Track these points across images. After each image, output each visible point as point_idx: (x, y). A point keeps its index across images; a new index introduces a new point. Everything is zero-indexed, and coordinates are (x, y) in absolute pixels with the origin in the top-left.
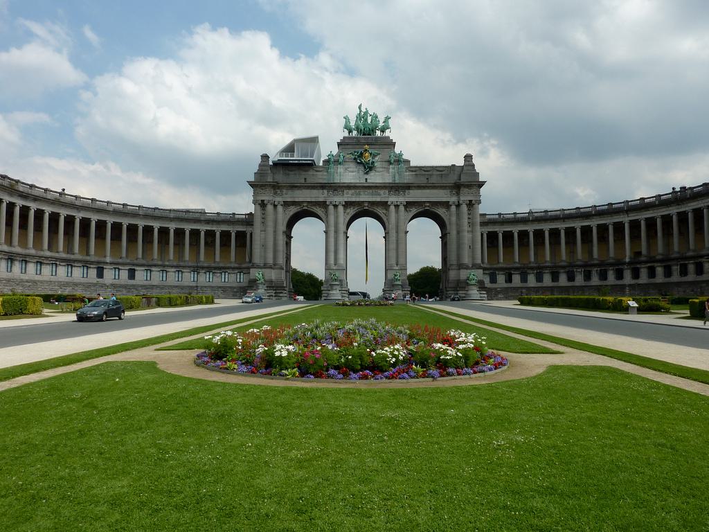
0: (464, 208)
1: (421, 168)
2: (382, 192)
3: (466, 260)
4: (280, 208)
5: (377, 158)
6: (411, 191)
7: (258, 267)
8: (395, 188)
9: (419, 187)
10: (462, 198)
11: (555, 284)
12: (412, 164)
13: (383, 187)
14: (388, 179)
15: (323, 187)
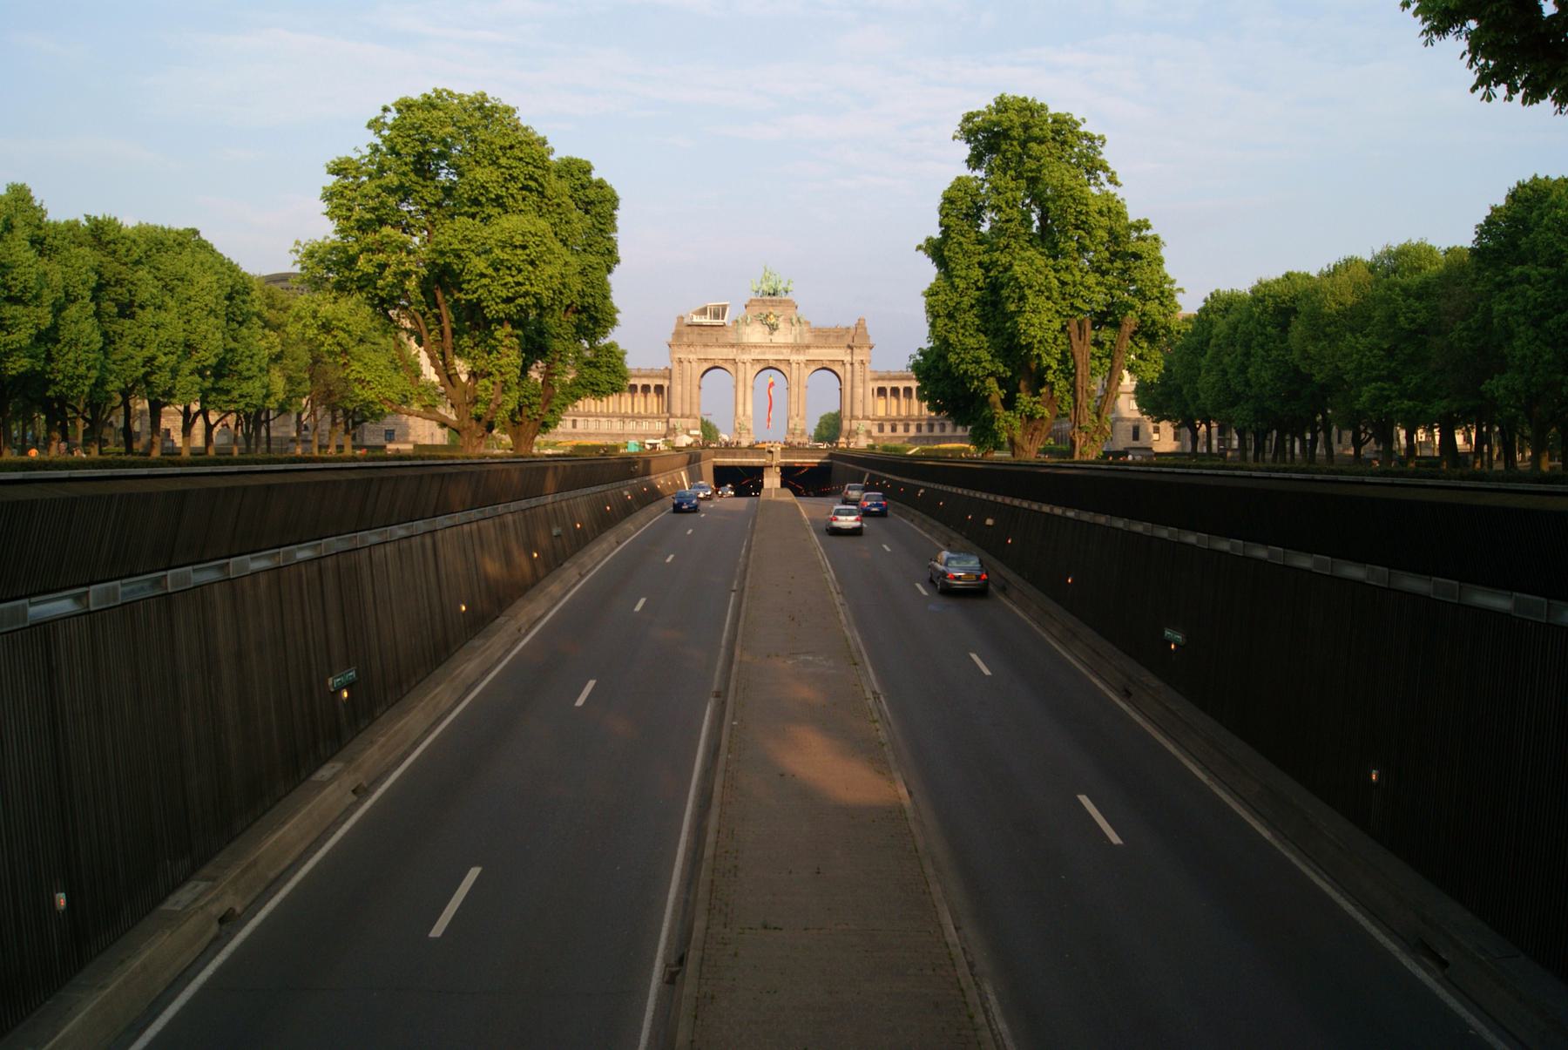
0: (857, 366)
1: (819, 330)
2: (785, 351)
3: (859, 412)
4: (694, 364)
5: (781, 319)
6: (811, 351)
7: (676, 417)
8: (797, 347)
9: (817, 347)
10: (855, 358)
11: (930, 434)
12: (813, 325)
13: (787, 346)
14: (790, 340)
15: (733, 346)
